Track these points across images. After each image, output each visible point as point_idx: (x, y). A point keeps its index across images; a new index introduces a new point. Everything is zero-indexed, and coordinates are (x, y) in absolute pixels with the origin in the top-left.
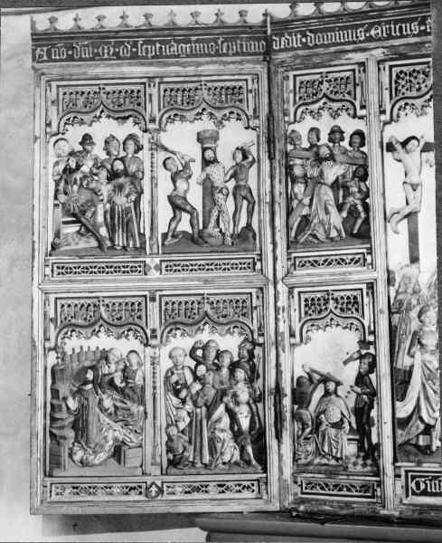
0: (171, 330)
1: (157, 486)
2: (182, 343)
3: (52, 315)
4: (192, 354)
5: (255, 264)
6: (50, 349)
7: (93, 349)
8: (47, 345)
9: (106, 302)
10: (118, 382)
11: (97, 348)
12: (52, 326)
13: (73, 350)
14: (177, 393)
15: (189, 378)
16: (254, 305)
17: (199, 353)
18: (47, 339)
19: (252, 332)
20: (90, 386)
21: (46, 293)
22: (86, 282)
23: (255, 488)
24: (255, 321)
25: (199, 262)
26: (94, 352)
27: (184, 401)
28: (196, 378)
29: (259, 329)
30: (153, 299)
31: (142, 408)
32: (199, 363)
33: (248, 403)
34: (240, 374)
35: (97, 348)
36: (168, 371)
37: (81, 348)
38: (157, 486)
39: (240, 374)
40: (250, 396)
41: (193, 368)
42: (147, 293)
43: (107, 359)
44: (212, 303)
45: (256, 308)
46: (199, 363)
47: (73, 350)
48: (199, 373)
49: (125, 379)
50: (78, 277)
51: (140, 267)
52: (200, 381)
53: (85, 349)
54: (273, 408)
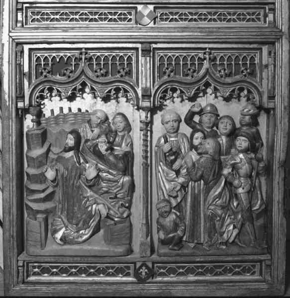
0: (166, 91)
1: (147, 267)
2: (178, 107)
3: (26, 69)
4: (189, 119)
5: (266, 16)
6: (26, 111)
7: (75, 110)
8: (20, 105)
10: (103, 148)
11: (80, 110)
12: (26, 83)
13: (52, 111)
14: (170, 164)
15: (184, 146)
16: (264, 63)
17: (196, 119)
18: (20, 97)
19: (260, 94)
20: (71, 153)
21: (17, 44)
22: (65, 30)
23: (257, 269)
24: (265, 82)
25: (200, 11)
26: (76, 114)
27: (178, 172)
28: (192, 147)
29: (269, 91)
30: (146, 52)
31: (127, 179)
32: (195, 130)
33: (250, 176)
34: (242, 142)
35: (80, 110)
36: (159, 139)
37: (61, 109)
38: (147, 267)
39: (242, 142)
40: (252, 169)
41: (189, 135)
43: (89, 122)
44: (215, 58)
45: (267, 66)
46: (195, 130)
47: (52, 111)
48: (196, 142)
49: (111, 149)
50: (56, 24)
51: (130, 14)
52: (196, 150)
53: (66, 111)
54: (282, 184)
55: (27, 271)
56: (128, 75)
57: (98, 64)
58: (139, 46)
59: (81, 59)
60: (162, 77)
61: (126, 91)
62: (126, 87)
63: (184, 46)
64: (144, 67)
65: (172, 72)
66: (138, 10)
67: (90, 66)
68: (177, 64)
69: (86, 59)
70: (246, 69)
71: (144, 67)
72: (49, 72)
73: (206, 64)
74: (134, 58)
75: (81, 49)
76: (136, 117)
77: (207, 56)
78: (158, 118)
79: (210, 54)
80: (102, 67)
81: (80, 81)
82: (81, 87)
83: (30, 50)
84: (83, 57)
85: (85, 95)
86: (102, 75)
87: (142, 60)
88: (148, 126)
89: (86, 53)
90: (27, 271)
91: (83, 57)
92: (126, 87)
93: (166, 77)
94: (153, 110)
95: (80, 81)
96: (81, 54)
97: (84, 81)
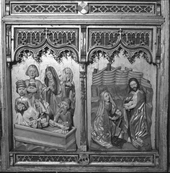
9: (49, 33)
42: (79, 27)
55: (16, 159)
56: (73, 43)
57: (56, 37)
58: (79, 27)
59: (45, 34)
60: (94, 45)
61: (71, 52)
62: (72, 50)
63: (104, 27)
64: (83, 40)
65: (99, 42)
66: (78, 5)
67: (51, 38)
68: (103, 37)
69: (48, 34)
70: (144, 41)
71: (83, 40)
72: (25, 41)
73: (120, 38)
74: (76, 35)
75: (45, 28)
76: (77, 68)
77: (120, 33)
78: (91, 69)
79: (122, 31)
80: (58, 38)
81: (45, 46)
82: (44, 50)
83: (15, 28)
84: (46, 33)
85: (47, 54)
86: (58, 43)
87: (81, 35)
88: (84, 74)
89: (48, 31)
90: (16, 159)
91: (46, 33)
92: (72, 50)
93: (96, 45)
94: (86, 64)
95: (45, 46)
96: (45, 31)
97: (47, 47)
